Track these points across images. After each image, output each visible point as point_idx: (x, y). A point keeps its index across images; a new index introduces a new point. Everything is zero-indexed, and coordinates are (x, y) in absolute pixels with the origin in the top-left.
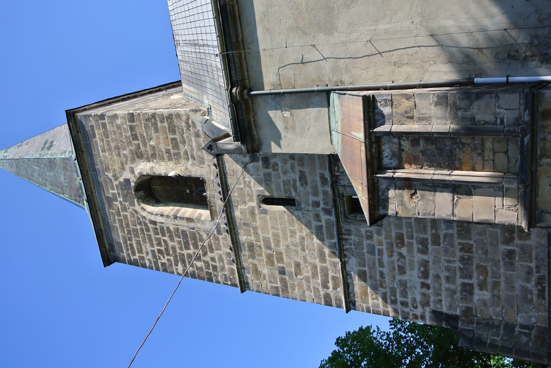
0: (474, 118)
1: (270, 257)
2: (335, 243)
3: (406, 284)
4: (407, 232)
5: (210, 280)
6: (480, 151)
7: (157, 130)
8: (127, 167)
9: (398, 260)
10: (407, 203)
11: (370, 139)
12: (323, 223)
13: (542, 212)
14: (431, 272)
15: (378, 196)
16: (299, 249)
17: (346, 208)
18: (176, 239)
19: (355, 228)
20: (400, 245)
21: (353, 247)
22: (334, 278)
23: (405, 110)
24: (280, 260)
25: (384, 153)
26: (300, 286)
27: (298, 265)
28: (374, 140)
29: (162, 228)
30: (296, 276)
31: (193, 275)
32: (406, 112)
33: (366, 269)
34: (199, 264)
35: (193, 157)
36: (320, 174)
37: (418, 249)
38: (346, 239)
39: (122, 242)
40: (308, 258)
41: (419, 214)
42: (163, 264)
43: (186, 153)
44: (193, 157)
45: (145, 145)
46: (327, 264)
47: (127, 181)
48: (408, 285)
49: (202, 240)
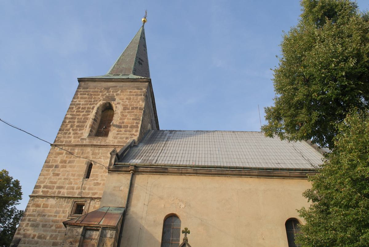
1: (65, 162)
2: (64, 195)
3: (37, 227)
4: (62, 231)
5: (60, 130)
7: (133, 119)
8: (121, 101)
9: (49, 224)
12: (75, 191)
14: (40, 240)
16: (65, 177)
17: (80, 202)
18: (83, 117)
19: (69, 205)
20: (57, 226)
21: (61, 203)
22: (48, 192)
23: (107, 243)
24: (63, 167)
27: (58, 175)
28: (98, 228)
29: (90, 111)
30: (53, 173)
31: (64, 122)
33: (49, 208)
34: (69, 126)
35: (118, 134)
36: (97, 193)
37: (53, 235)
38: (65, 201)
39: (88, 90)
40: (60, 181)
42: (73, 108)
43: (121, 131)
44: (118, 134)
45: (128, 112)
46: (55, 189)
47: (114, 100)
48: (36, 228)
49: (80, 130)
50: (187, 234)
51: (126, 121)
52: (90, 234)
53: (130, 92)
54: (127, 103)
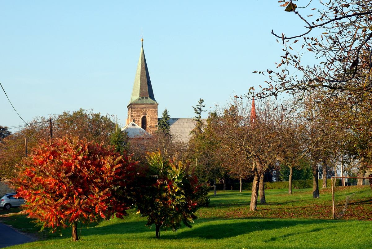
45: (153, 121)
51: (152, 124)
53: (152, 110)
54: (151, 116)
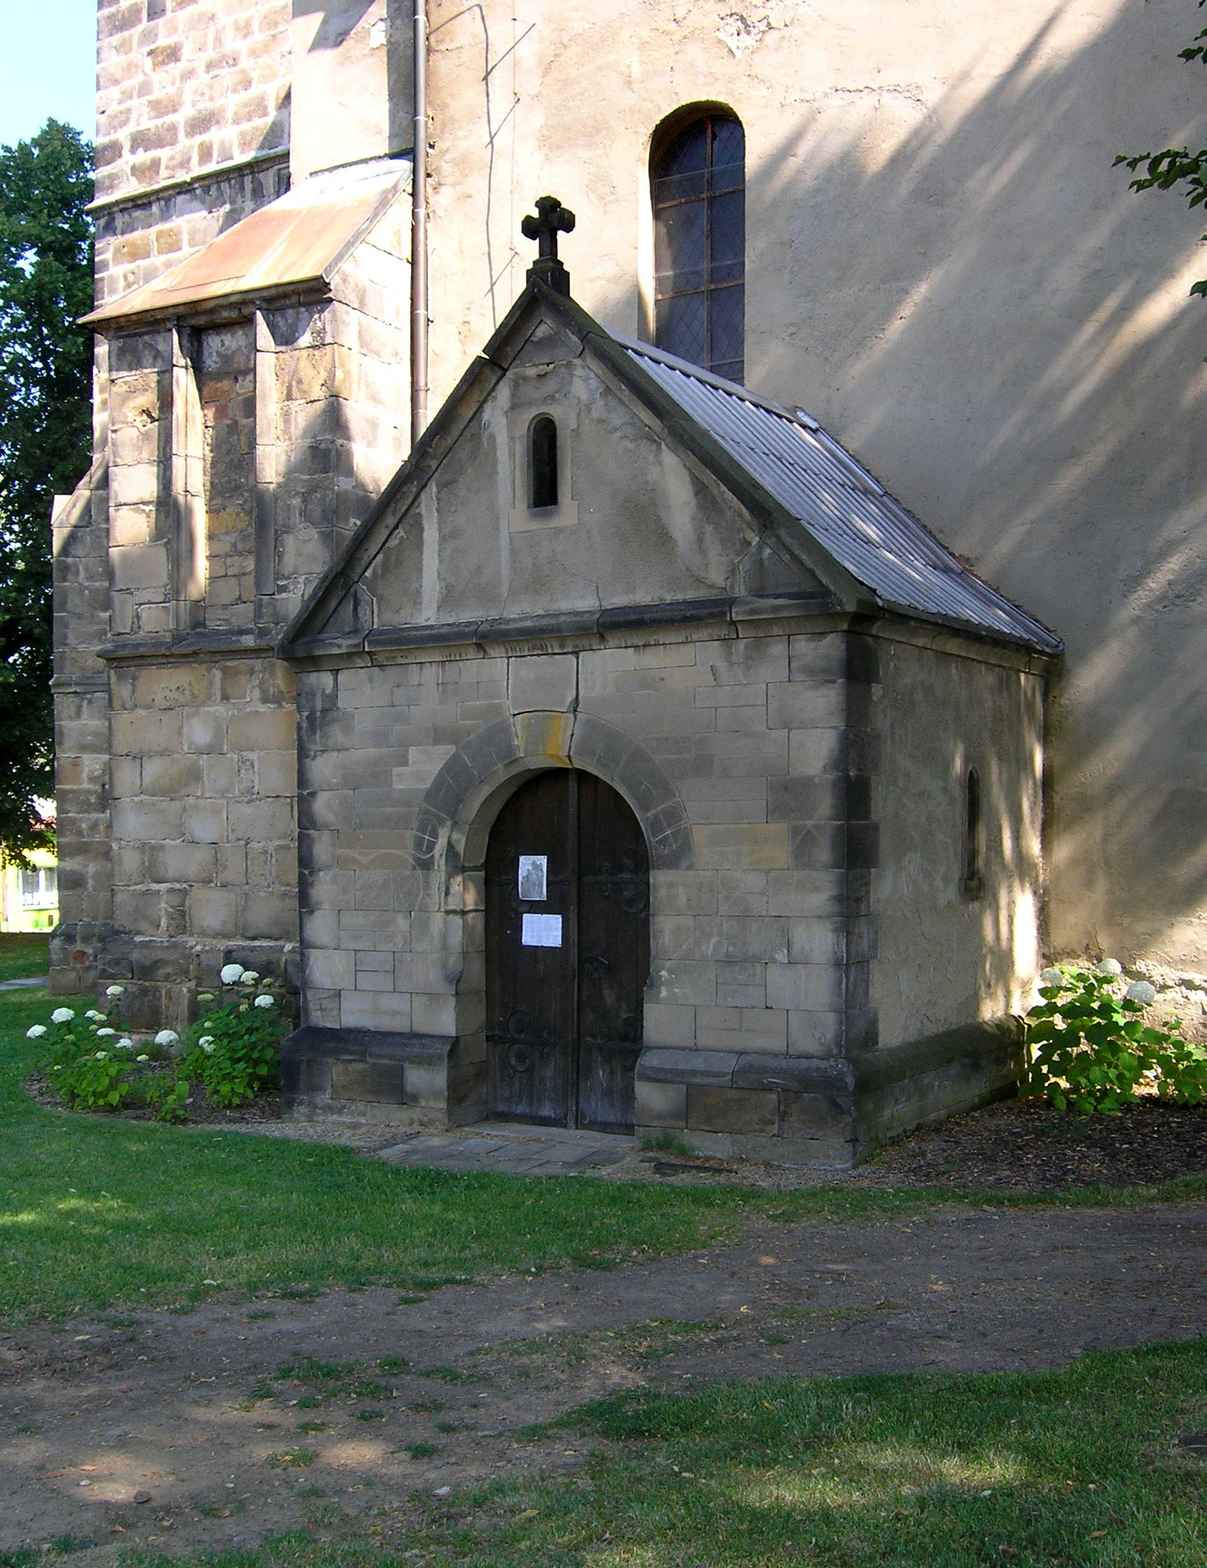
0: (287, 533)
6: (240, 546)
10: (132, 404)
11: (244, 303)
13: (134, 679)
15: (141, 335)
16: (210, 54)
22: (155, 165)
25: (229, 335)
26: (130, 68)
27: (173, 54)
28: (246, 311)
30: (149, 54)
32: (300, 382)
38: (242, 188)
40: (190, 86)
41: (114, 431)
46: (184, 142)
50: (561, 234)
52: (222, 350)
